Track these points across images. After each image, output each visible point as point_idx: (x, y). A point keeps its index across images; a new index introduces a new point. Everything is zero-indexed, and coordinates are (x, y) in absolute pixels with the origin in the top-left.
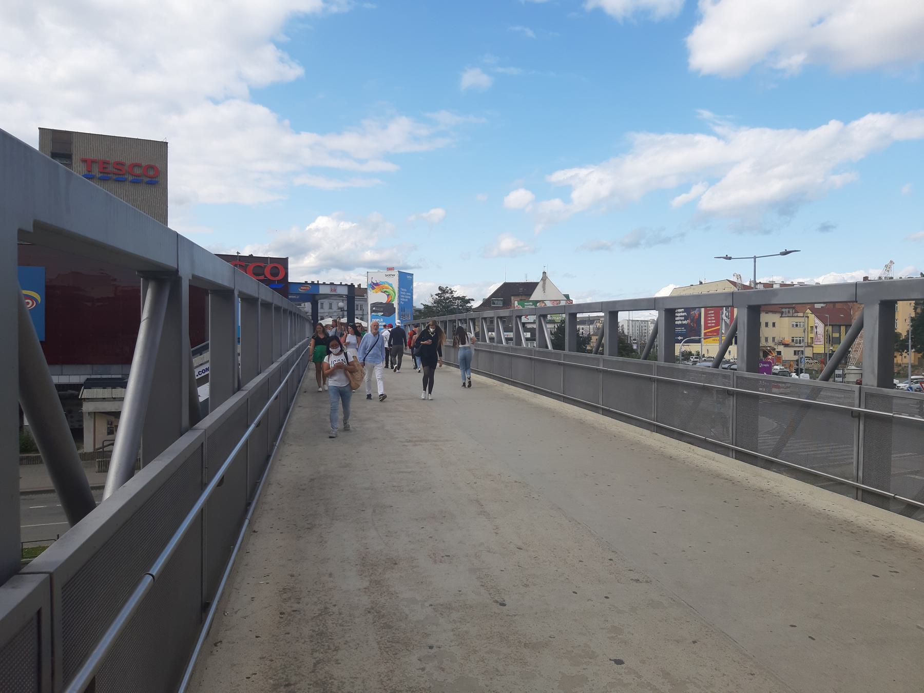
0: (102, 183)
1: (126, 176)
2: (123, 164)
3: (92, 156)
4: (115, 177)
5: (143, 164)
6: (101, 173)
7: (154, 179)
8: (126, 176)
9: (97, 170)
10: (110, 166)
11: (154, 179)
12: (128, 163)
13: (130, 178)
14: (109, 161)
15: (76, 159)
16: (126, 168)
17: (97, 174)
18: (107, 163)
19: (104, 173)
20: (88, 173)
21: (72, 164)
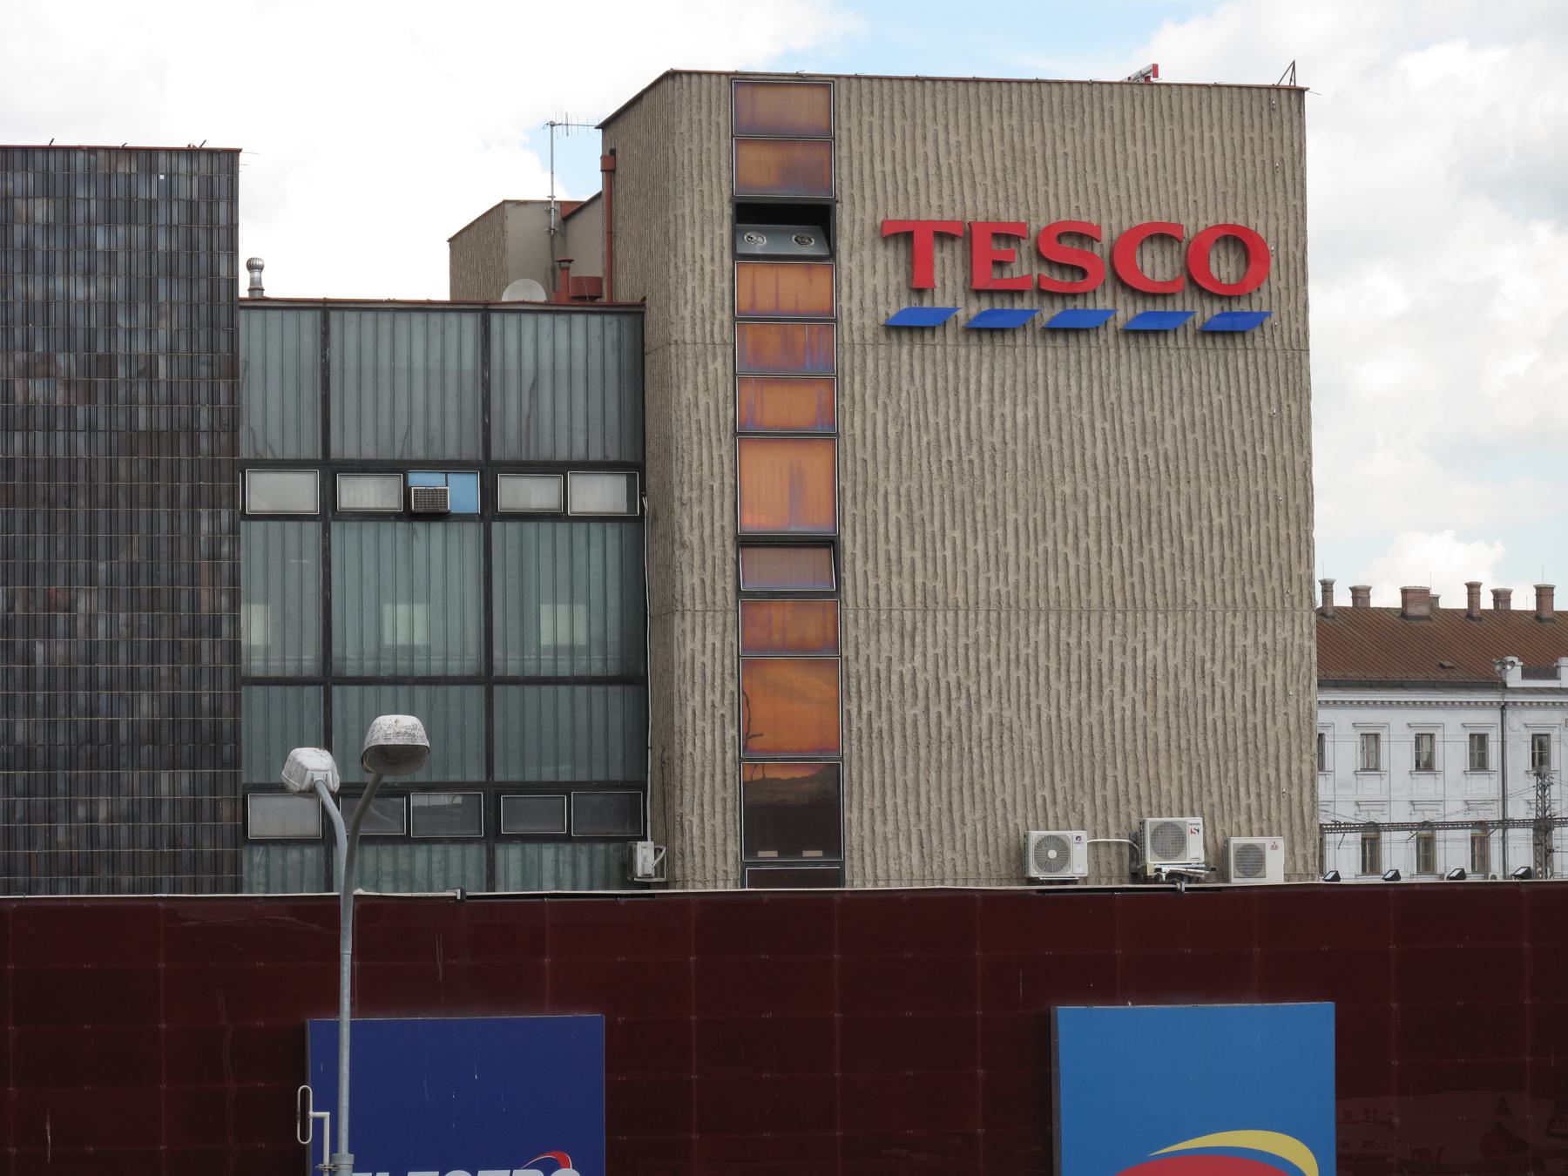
0: (986, 349)
1: (1103, 303)
2: (1084, 235)
3: (934, 206)
4: (1049, 312)
5: (1193, 224)
6: (978, 293)
7: (1242, 307)
8: (1103, 303)
9: (960, 279)
10: (1024, 251)
11: (1242, 307)
12: (1111, 227)
13: (1126, 311)
14: (1018, 224)
15: (853, 222)
16: (1101, 250)
17: (961, 304)
18: (1008, 235)
19: (991, 293)
20: (915, 301)
21: (832, 254)
